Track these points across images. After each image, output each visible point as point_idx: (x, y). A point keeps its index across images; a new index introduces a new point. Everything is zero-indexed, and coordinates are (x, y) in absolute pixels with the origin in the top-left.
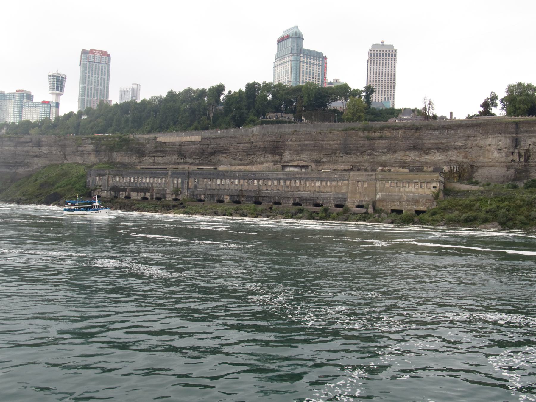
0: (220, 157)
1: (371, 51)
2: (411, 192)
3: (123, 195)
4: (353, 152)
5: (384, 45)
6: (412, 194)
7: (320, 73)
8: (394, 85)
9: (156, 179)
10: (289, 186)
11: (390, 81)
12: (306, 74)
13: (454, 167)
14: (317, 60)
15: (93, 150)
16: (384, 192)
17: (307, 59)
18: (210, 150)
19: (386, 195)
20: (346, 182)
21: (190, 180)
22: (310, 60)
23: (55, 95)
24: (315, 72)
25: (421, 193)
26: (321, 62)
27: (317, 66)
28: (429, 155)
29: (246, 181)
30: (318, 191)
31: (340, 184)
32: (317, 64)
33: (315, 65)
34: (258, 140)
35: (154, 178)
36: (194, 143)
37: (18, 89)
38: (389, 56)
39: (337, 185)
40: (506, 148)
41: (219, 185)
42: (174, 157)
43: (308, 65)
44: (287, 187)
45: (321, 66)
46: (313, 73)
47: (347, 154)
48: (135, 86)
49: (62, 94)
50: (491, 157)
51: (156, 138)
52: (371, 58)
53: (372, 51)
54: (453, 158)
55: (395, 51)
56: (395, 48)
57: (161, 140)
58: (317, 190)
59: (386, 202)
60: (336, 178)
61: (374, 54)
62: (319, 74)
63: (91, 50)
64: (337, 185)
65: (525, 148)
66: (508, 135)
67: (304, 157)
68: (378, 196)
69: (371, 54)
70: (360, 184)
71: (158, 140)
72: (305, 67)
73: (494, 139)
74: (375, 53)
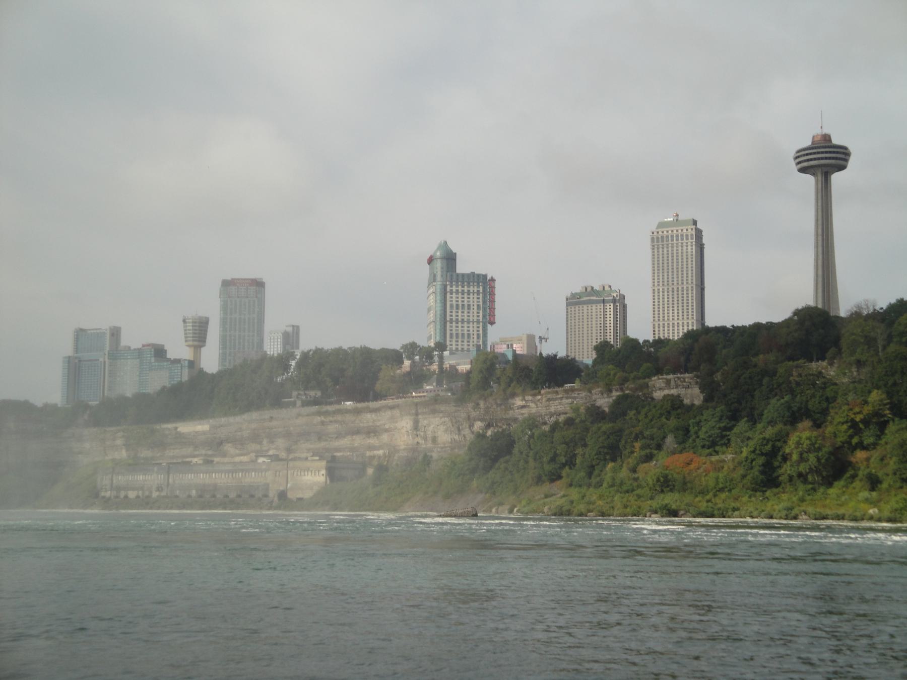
3: (122, 494)
7: (481, 303)
11: (670, 283)
12: (457, 308)
15: (124, 445)
17: (457, 286)
21: (171, 476)
22: (463, 287)
23: (192, 349)
24: (471, 303)
26: (481, 287)
27: (475, 294)
29: (208, 475)
32: (475, 291)
33: (471, 294)
36: (204, 433)
37: (145, 343)
38: (682, 239)
43: (460, 295)
45: (481, 295)
46: (469, 305)
48: (290, 329)
49: (204, 346)
51: (176, 428)
53: (655, 233)
62: (478, 306)
63: (233, 280)
68: (289, 485)
69: (653, 239)
72: (454, 299)
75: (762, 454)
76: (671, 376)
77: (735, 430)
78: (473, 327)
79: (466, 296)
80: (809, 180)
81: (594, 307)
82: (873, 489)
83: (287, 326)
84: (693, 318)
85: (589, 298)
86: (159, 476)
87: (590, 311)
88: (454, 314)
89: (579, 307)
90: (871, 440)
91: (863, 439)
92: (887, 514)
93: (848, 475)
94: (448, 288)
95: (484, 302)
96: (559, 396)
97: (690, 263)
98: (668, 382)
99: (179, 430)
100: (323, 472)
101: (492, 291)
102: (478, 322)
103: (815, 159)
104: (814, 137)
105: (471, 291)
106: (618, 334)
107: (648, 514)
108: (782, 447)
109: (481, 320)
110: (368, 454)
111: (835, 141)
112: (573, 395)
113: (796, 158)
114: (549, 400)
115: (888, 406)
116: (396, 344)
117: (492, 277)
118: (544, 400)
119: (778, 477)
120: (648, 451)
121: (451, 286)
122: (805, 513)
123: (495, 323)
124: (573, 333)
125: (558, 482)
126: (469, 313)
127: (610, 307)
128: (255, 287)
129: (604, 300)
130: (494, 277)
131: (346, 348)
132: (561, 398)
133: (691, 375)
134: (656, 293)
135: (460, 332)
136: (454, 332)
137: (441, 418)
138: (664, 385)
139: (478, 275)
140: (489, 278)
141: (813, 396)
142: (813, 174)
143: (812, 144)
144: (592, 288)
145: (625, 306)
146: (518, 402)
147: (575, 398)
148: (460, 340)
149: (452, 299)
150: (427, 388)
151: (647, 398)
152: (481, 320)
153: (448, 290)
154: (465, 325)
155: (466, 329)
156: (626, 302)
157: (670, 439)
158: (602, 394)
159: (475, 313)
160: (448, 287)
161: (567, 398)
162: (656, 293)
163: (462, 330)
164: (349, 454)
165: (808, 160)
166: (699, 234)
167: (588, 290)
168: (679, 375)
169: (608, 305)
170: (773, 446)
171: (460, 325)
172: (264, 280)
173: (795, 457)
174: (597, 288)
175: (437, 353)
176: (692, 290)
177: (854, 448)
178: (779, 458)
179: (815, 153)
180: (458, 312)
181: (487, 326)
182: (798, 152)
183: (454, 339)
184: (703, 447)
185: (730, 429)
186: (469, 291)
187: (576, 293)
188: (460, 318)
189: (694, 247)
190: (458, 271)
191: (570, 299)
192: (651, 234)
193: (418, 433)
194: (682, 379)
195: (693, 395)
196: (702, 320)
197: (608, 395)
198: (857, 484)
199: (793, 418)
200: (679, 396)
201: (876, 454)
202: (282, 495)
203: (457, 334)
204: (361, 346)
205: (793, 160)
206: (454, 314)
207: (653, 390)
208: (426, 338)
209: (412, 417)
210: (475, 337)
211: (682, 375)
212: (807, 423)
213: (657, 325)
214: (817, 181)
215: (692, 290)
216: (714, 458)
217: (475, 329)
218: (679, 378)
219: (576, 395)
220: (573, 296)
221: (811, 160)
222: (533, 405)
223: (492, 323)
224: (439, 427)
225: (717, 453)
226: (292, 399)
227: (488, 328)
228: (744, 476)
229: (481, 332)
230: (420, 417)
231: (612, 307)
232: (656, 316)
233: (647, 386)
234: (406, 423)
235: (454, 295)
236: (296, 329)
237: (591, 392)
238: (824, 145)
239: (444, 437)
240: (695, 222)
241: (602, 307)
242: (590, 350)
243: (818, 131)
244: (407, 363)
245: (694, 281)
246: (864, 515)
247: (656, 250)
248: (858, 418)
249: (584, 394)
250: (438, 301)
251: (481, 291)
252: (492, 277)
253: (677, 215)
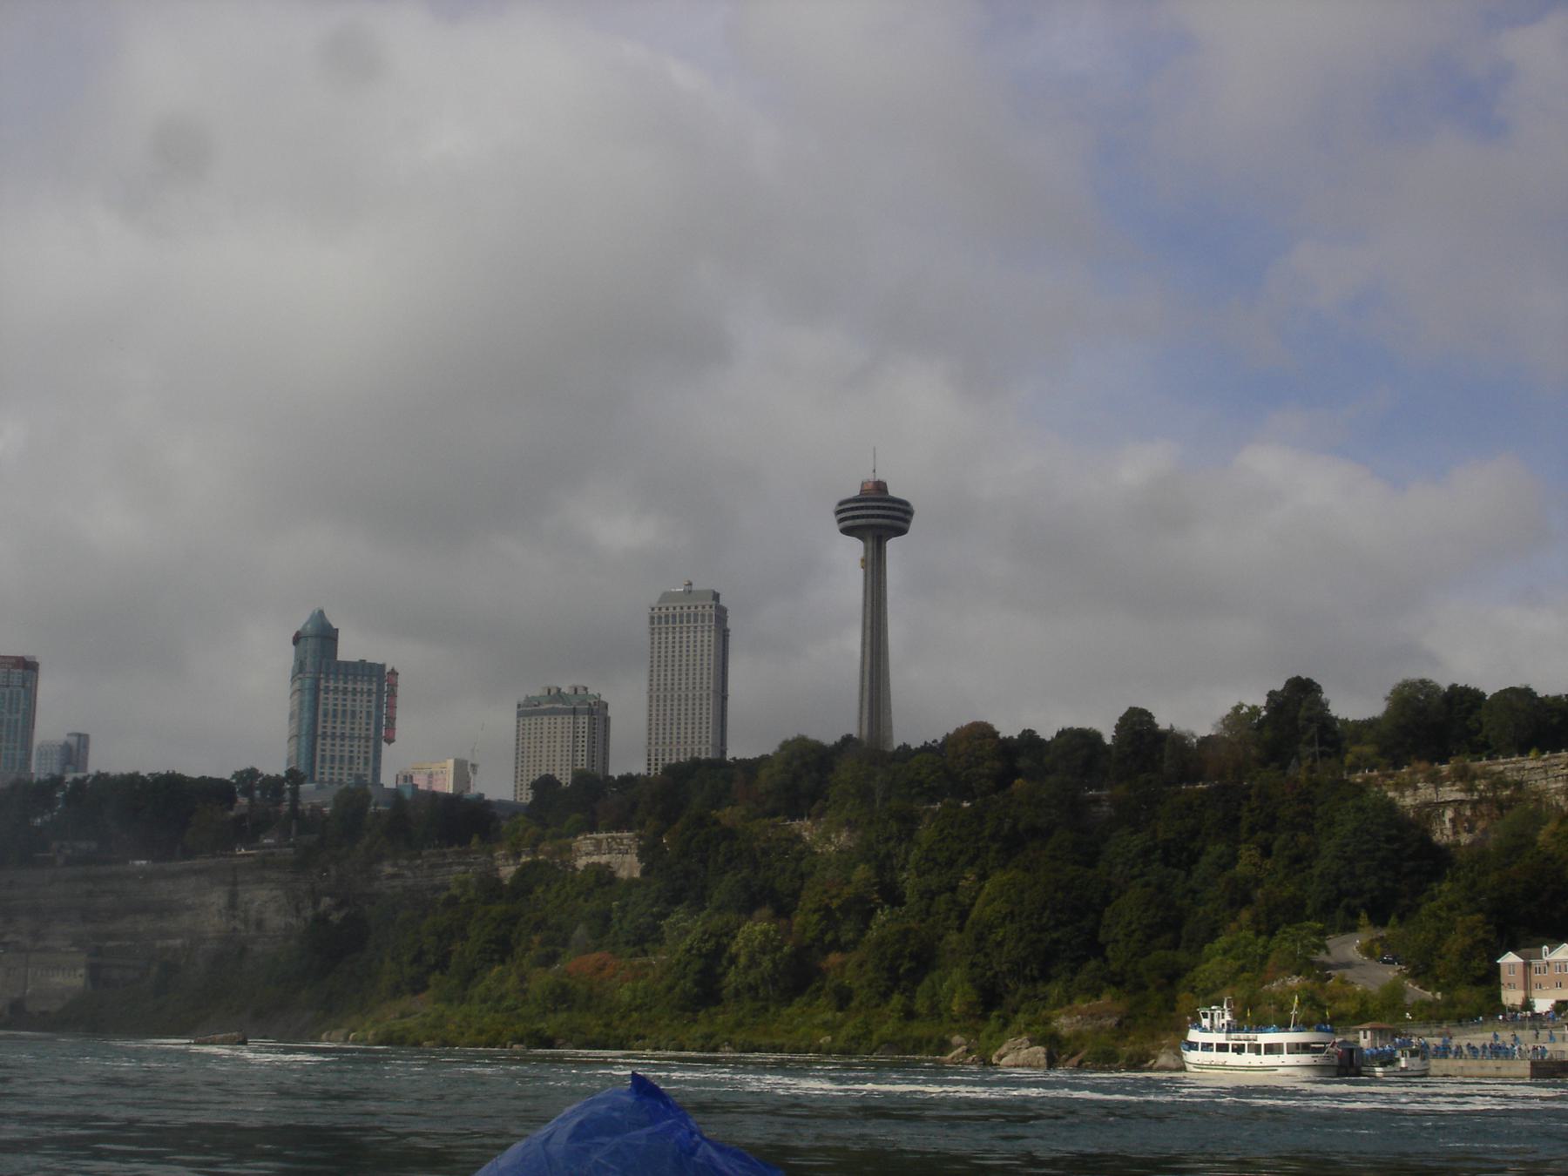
1: (653, 609)
5: (690, 592)
7: (373, 710)
12: (335, 716)
17: (337, 680)
27: (365, 695)
33: (359, 695)
43: (340, 696)
45: (374, 695)
48: (73, 741)
52: (653, 629)
53: (656, 610)
61: (660, 618)
69: (652, 618)
72: (331, 701)
74: (663, 616)
75: (700, 955)
76: (603, 835)
77: (671, 920)
78: (359, 746)
79: (349, 696)
80: (854, 548)
81: (559, 720)
82: (840, 1009)
83: (69, 735)
84: (707, 742)
85: (551, 706)
87: (552, 726)
88: (329, 725)
89: (536, 719)
90: (851, 935)
91: (839, 934)
92: (840, 1043)
93: (813, 987)
94: (323, 684)
95: (379, 707)
96: (447, 861)
97: (705, 658)
98: (598, 844)
100: (82, 971)
101: (393, 690)
102: (367, 739)
103: (863, 517)
104: (863, 484)
105: (359, 690)
106: (595, 763)
107: (509, 1043)
108: (729, 945)
109: (372, 736)
110: (158, 944)
111: (893, 492)
112: (468, 860)
113: (838, 513)
114: (432, 866)
115: (875, 888)
116: (223, 770)
117: (393, 670)
118: (425, 866)
119: (721, 990)
120: (549, 949)
121: (327, 681)
122: (730, 1044)
123: (394, 741)
124: (525, 759)
125: (423, 996)
126: (353, 723)
127: (583, 720)
128: (20, 671)
129: (574, 709)
130: (396, 669)
131: (145, 775)
132: (450, 864)
133: (631, 834)
134: (655, 701)
135: (337, 754)
136: (328, 754)
137: (271, 890)
138: (592, 848)
139: (372, 666)
140: (388, 669)
141: (783, 870)
142: (860, 538)
143: (861, 494)
144: (559, 690)
145: (607, 720)
146: (387, 869)
147: (470, 864)
148: (337, 765)
149: (328, 701)
150: (265, 841)
151: (566, 867)
152: (372, 736)
153: (322, 687)
154: (347, 742)
155: (347, 749)
156: (609, 714)
157: (580, 931)
158: (507, 859)
159: (364, 725)
160: (322, 682)
161: (459, 864)
162: (655, 701)
163: (341, 751)
164: (128, 943)
165: (853, 517)
166: (721, 615)
167: (552, 693)
168: (614, 834)
169: (581, 717)
170: (718, 943)
171: (338, 742)
172: (37, 660)
173: (743, 960)
174: (565, 689)
175: (288, 786)
176: (708, 699)
177: (827, 950)
178: (725, 962)
179: (862, 508)
180: (335, 722)
181: (381, 745)
182: (841, 504)
183: (328, 765)
184: (627, 943)
185: (665, 916)
186: (354, 689)
187: (533, 697)
188: (338, 732)
189: (713, 634)
190: (340, 658)
191: (524, 706)
192: (650, 611)
194: (618, 840)
195: (628, 866)
196: (722, 745)
197: (515, 860)
198: (822, 1001)
199: (749, 906)
200: (608, 865)
201: (854, 958)
202: (17, 1007)
203: (333, 757)
205: (833, 515)
206: (329, 725)
207: (576, 856)
208: (274, 766)
210: (362, 761)
211: (619, 834)
212: (766, 911)
213: (653, 752)
214: (866, 549)
215: (708, 699)
216: (637, 961)
217: (362, 749)
218: (613, 838)
219: (472, 860)
220: (529, 700)
221: (858, 517)
222: (408, 873)
223: (390, 740)
224: (267, 905)
225: (645, 953)
226: (51, 854)
227: (383, 749)
228: (670, 989)
229: (371, 755)
230: (239, 888)
231: (586, 720)
232: (654, 736)
233: (570, 850)
234: (217, 898)
235: (331, 695)
236: (83, 740)
237: (492, 857)
238: (876, 496)
239: (276, 921)
240: (716, 596)
241: (572, 721)
242: (525, 787)
243: (870, 477)
244: (243, 801)
245: (712, 686)
246: (810, 1046)
247: (656, 636)
248: (835, 904)
249: (483, 858)
250: (306, 704)
251: (374, 690)
252: (393, 670)
253: (690, 584)
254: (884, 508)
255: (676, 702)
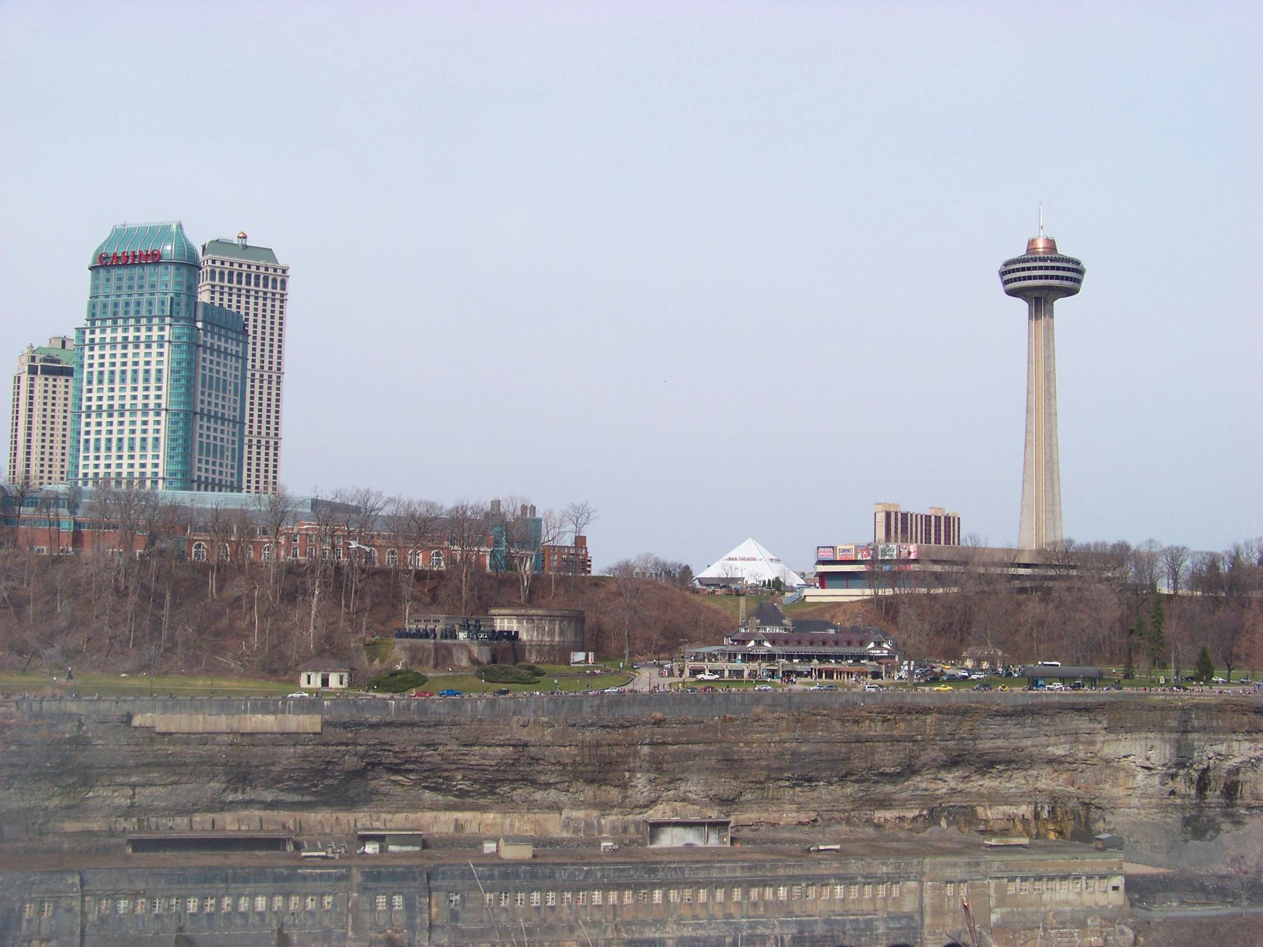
0: (382, 782)
2: (1067, 903)
4: (824, 774)
5: (246, 247)
6: (1068, 908)
8: (279, 377)
9: (294, 900)
10: (762, 903)
13: (1042, 808)
14: (213, 334)
16: (1006, 906)
18: (351, 762)
19: (1012, 912)
20: (913, 884)
25: (1088, 904)
28: (988, 775)
30: (842, 911)
31: (895, 891)
34: (549, 738)
35: (287, 896)
39: (889, 892)
40: (1164, 765)
41: (538, 908)
42: (212, 784)
44: (755, 904)
47: (809, 780)
50: (1130, 785)
51: (129, 717)
54: (1042, 784)
55: (284, 271)
56: (282, 262)
57: (148, 723)
58: (838, 908)
59: (1015, 932)
60: (888, 873)
64: (889, 892)
65: (1201, 767)
66: (1167, 736)
67: (687, 789)
70: (950, 889)
71: (137, 721)
73: (1138, 743)
74: (226, 272)
86: (381, 900)
99: (137, 721)
103: (1057, 278)
142: (1025, 298)
193: (1181, 772)
204: (496, 503)
209: (1174, 736)
253: (245, 237)
254: (1058, 268)
255: (266, 384)
